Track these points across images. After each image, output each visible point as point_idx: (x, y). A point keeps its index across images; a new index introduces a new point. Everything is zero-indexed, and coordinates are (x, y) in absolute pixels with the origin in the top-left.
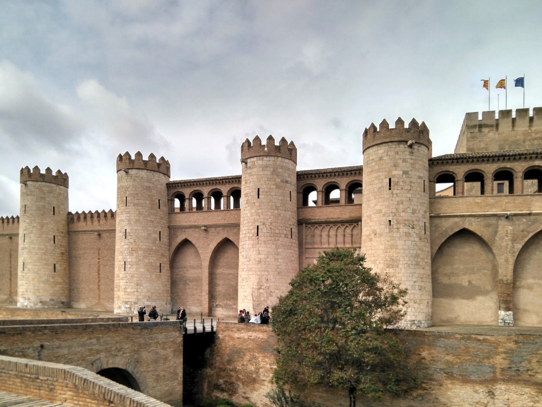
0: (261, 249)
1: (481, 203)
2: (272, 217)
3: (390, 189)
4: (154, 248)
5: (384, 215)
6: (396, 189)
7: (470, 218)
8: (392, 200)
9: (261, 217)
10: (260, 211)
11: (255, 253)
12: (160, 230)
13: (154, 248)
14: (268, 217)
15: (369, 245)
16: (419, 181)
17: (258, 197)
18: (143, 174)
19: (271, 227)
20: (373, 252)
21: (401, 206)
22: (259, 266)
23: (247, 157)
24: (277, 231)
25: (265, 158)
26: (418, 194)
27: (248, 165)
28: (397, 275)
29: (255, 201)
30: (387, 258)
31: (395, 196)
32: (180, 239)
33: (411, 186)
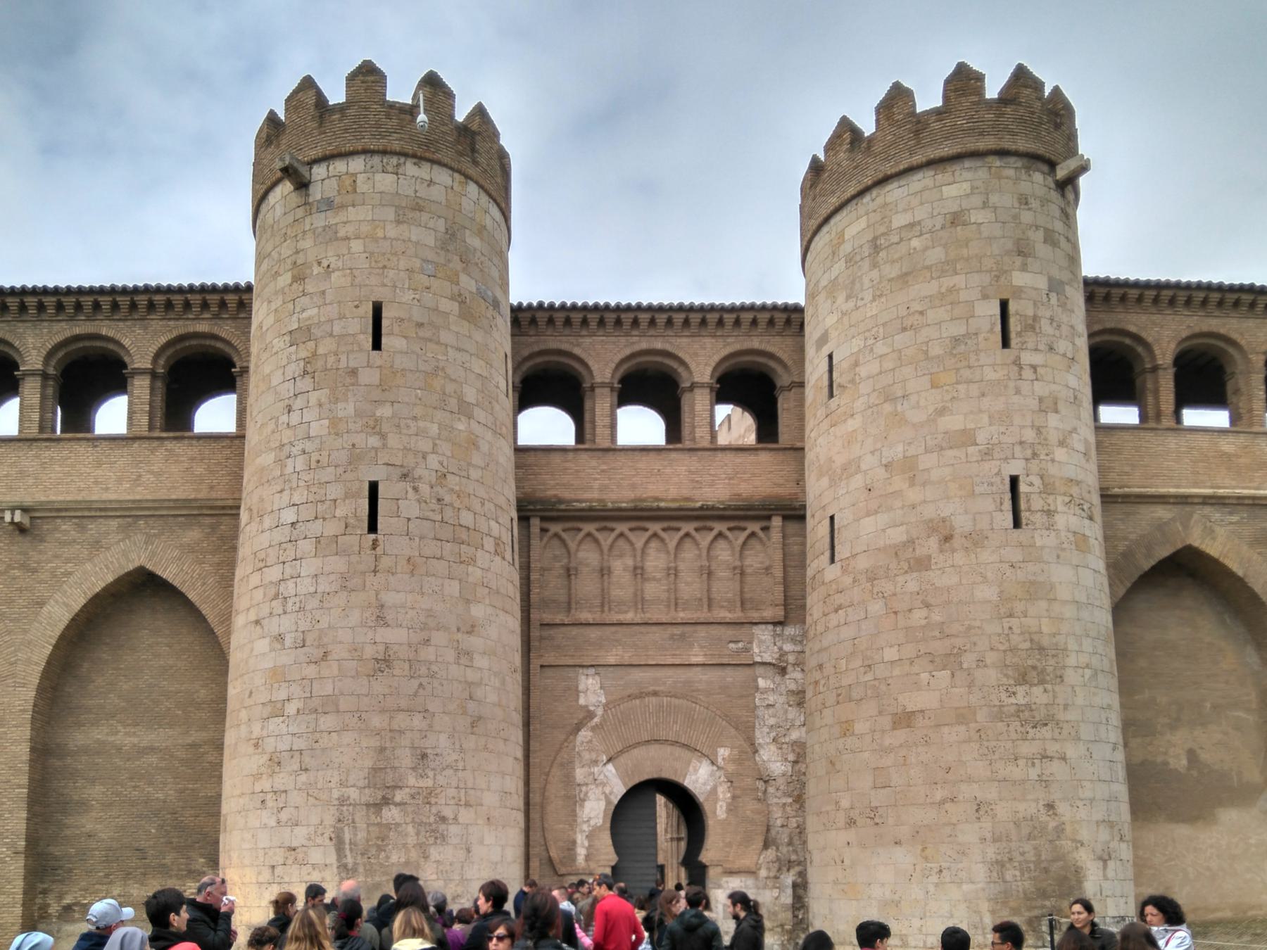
0: (389, 598)
1: (1238, 456)
7: (1207, 510)
9: (393, 441)
10: (385, 411)
11: (355, 617)
14: (424, 445)
15: (912, 586)
17: (377, 345)
19: (442, 492)
20: (936, 617)
22: (379, 686)
23: (313, 154)
27: (316, 192)
29: (357, 360)
30: (1015, 639)
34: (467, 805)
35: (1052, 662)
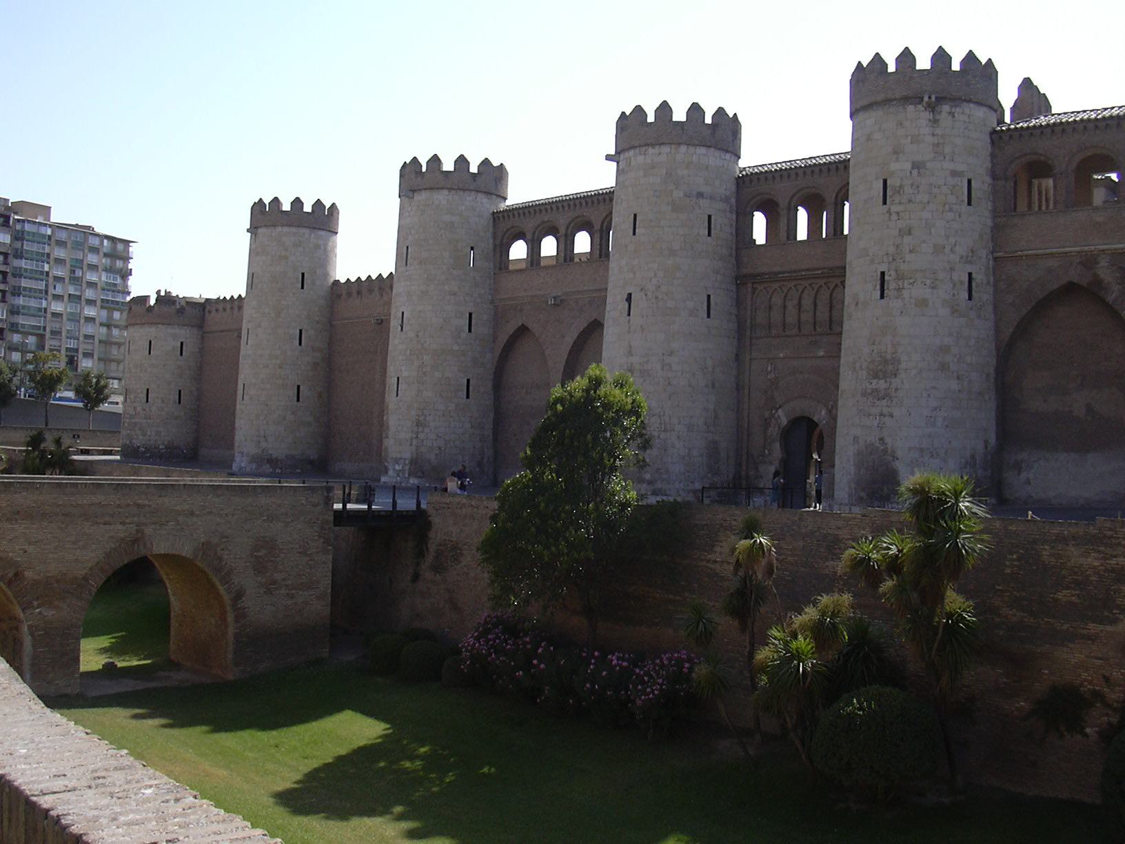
2: (661, 274)
3: (885, 203)
4: (456, 348)
5: (872, 261)
6: (897, 201)
8: (888, 227)
12: (470, 309)
13: (456, 348)
18: (442, 197)
21: (907, 239)
25: (651, 150)
26: (951, 210)
28: (893, 394)
31: (894, 217)
32: (510, 328)
33: (930, 194)
34: (665, 430)
35: (891, 367)
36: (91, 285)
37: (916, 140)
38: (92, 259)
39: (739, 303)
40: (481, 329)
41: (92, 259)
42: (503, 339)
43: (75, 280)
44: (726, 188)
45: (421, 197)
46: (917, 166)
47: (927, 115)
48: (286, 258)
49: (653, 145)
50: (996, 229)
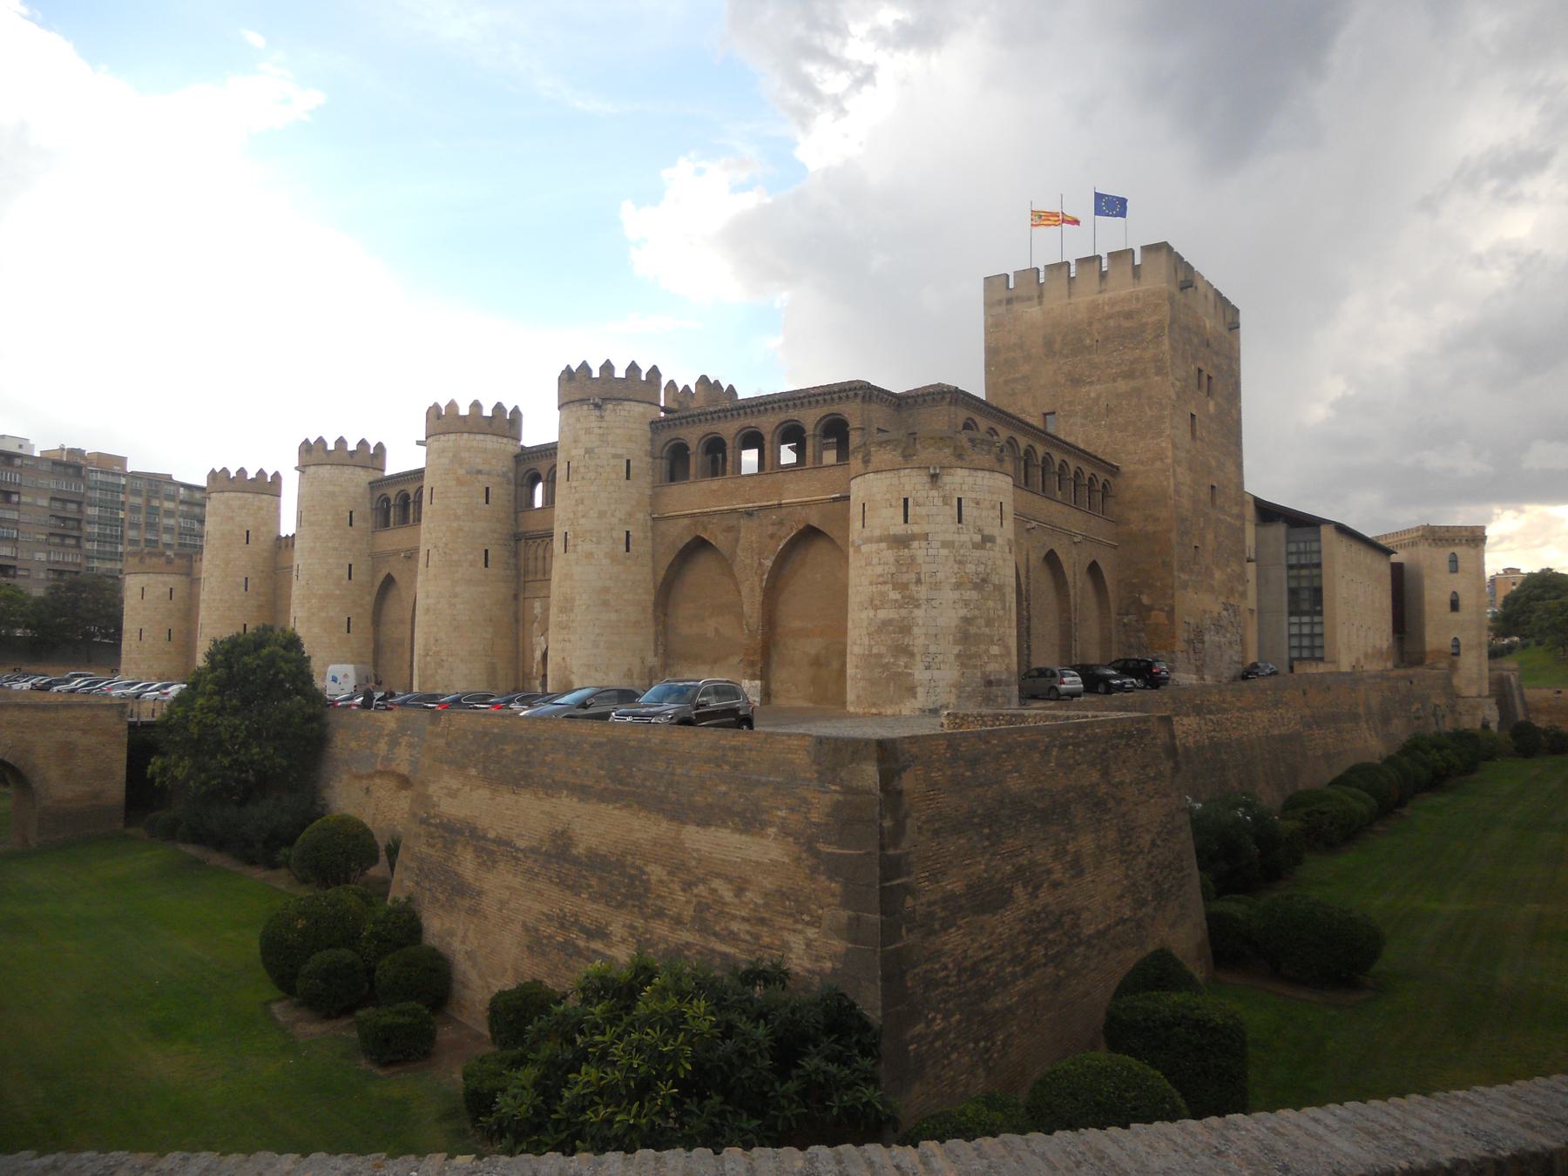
16: (613, 462)
18: (325, 471)
21: (581, 508)
24: (455, 557)
25: (442, 438)
32: (381, 577)
36: (168, 530)
37: (588, 431)
38: (168, 505)
39: (516, 554)
40: (361, 574)
41: (168, 505)
42: (378, 583)
43: (151, 526)
44: (504, 465)
45: (312, 469)
46: (588, 451)
47: (597, 413)
48: (232, 518)
49: (444, 433)
50: (654, 498)
